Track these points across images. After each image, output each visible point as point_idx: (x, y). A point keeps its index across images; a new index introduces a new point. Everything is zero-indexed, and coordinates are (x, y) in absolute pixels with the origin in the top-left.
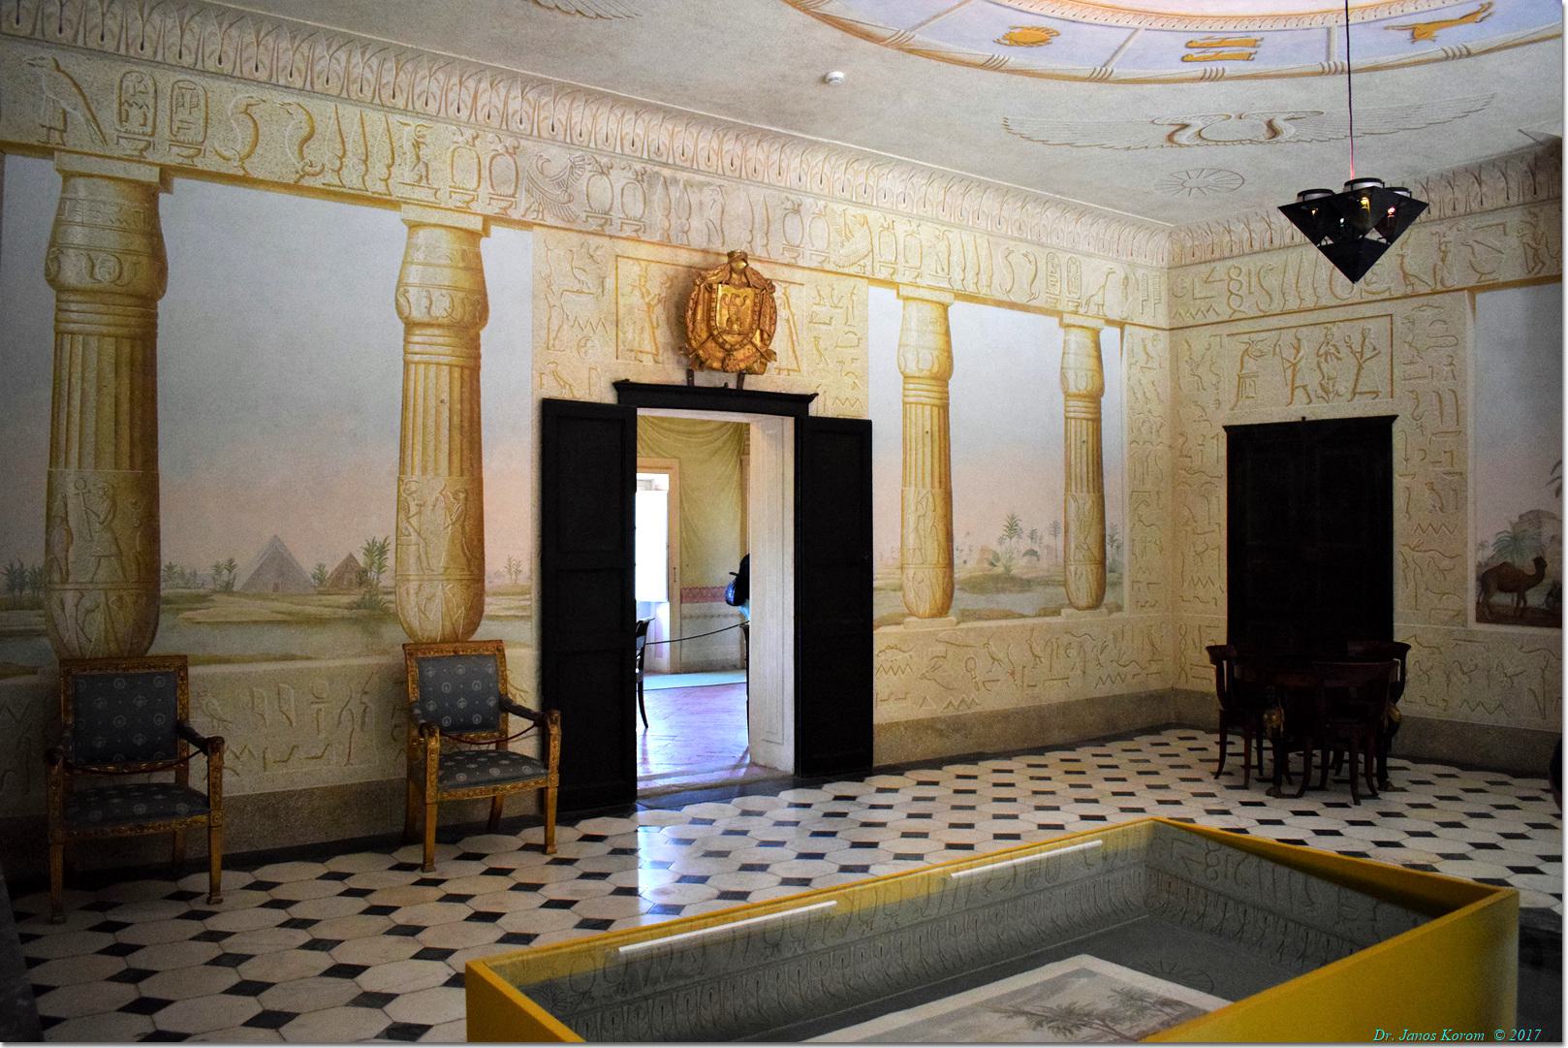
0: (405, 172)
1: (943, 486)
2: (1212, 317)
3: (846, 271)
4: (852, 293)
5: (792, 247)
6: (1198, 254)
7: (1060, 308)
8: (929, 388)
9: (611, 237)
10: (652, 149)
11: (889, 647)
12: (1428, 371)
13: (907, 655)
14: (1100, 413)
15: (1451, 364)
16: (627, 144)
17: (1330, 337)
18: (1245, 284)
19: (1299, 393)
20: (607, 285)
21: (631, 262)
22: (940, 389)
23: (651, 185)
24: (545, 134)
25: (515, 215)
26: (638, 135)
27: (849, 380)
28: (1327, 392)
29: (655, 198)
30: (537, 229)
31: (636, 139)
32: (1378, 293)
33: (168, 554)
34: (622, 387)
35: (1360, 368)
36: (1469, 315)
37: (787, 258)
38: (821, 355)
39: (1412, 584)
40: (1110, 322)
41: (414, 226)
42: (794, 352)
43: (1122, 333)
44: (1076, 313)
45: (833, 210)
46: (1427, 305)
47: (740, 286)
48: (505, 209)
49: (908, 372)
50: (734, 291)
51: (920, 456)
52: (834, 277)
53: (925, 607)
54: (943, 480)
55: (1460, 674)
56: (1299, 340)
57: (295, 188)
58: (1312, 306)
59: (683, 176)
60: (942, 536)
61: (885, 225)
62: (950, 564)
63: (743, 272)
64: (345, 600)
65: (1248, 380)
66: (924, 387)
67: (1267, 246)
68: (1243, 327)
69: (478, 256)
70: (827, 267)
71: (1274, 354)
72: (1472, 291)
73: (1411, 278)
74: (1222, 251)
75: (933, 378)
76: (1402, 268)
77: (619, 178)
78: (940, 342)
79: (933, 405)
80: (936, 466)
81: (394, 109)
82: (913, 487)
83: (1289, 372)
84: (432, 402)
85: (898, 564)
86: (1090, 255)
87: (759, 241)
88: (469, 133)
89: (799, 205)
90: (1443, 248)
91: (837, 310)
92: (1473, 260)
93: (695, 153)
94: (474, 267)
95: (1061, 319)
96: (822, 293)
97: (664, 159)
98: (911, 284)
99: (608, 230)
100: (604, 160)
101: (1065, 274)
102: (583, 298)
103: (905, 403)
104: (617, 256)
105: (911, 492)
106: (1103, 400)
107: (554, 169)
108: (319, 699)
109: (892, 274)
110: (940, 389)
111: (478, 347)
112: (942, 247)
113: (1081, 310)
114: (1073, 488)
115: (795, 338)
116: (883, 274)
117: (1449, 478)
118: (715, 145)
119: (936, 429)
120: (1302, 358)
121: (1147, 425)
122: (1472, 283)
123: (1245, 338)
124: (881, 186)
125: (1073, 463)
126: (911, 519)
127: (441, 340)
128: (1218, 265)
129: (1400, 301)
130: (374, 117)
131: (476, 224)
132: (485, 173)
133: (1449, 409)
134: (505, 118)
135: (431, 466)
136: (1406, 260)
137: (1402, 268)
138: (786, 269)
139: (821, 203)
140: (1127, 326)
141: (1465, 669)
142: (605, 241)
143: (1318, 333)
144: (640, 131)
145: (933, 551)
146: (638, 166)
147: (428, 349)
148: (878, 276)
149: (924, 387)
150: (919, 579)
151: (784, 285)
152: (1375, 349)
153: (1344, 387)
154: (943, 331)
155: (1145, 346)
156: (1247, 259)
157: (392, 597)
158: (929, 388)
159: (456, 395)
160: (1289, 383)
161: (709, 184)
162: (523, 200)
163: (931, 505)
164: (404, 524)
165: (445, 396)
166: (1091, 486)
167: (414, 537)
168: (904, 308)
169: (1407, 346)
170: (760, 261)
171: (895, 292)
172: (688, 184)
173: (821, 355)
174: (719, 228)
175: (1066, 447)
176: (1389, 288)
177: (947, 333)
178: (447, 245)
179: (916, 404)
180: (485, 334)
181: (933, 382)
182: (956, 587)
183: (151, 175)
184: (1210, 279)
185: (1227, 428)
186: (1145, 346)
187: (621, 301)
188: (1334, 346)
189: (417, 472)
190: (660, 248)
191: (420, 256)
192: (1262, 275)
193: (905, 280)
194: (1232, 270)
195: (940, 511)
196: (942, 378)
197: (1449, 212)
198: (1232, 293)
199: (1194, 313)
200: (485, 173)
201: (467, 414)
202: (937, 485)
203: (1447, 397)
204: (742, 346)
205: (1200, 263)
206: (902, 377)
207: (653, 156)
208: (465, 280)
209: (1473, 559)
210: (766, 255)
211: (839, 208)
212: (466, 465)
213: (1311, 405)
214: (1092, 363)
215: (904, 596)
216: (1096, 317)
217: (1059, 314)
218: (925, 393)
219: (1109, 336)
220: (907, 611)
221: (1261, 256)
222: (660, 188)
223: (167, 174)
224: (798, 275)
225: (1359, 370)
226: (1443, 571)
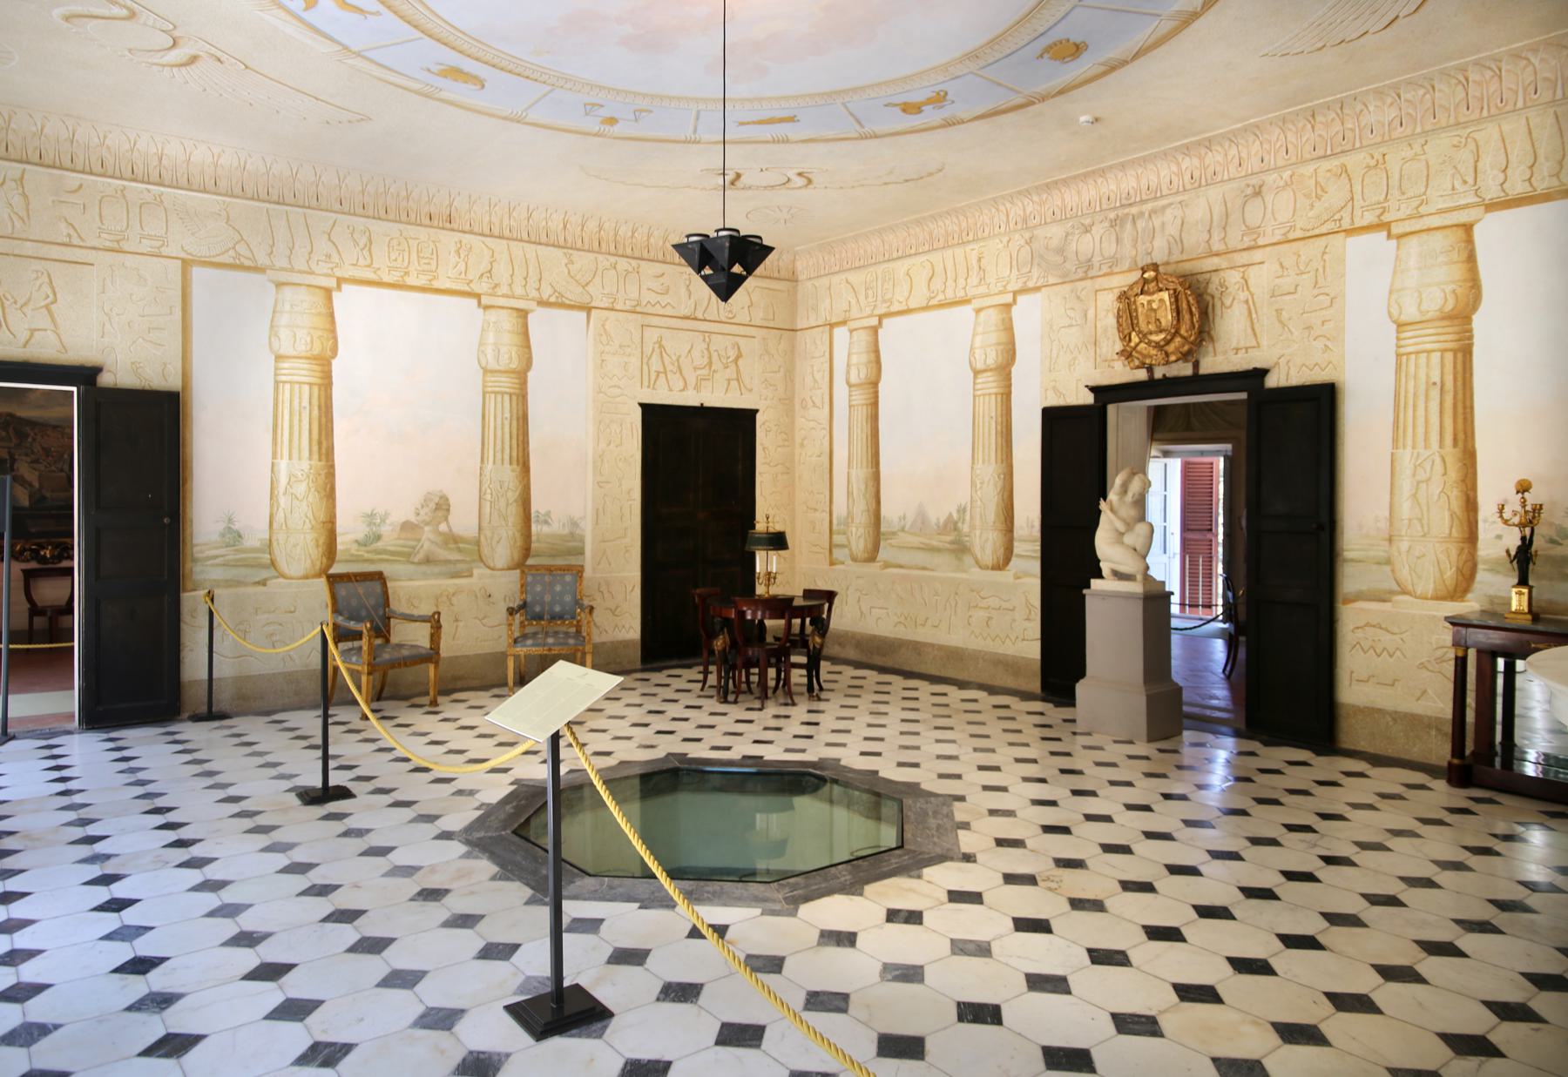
0: (974, 280)
1: (1461, 444)
3: (1317, 232)
4: (1324, 253)
5: (1251, 230)
8: (1440, 330)
9: (1092, 278)
10: (1123, 196)
11: (1368, 625)
13: (1397, 638)
16: (1104, 201)
20: (1089, 316)
21: (1106, 292)
22: (1456, 329)
23: (1122, 226)
24: (1048, 220)
25: (1031, 284)
26: (1112, 191)
27: (1319, 344)
29: (1125, 235)
30: (1043, 289)
31: (1111, 194)
33: (884, 511)
34: (1095, 390)
37: (1247, 242)
38: (1284, 325)
41: (978, 311)
42: (1253, 330)
45: (1302, 175)
47: (1153, 293)
48: (1025, 283)
49: (1404, 318)
50: (1148, 298)
51: (1421, 411)
52: (1302, 243)
53: (1427, 585)
54: (1461, 436)
57: (926, 308)
59: (1149, 206)
60: (1457, 505)
61: (1373, 163)
63: (1156, 279)
64: (948, 538)
66: (1432, 331)
69: (1011, 319)
70: (1291, 236)
75: (1443, 318)
77: (1098, 231)
78: (1458, 272)
79: (1444, 351)
81: (969, 242)
82: (1409, 449)
84: (987, 419)
85: (1387, 536)
87: (1216, 236)
88: (1005, 240)
89: (1260, 187)
91: (1305, 276)
93: (1159, 184)
94: (1009, 328)
96: (1284, 264)
97: (1132, 201)
98: (1410, 218)
99: (1091, 274)
100: (1087, 221)
102: (1074, 329)
104: (1097, 291)
107: (1054, 243)
108: (936, 594)
109: (1379, 216)
110: (1456, 329)
111: (1010, 379)
112: (1466, 156)
115: (1254, 316)
116: (1370, 218)
118: (1174, 168)
124: (1363, 124)
126: (1406, 486)
127: (991, 379)
130: (959, 251)
131: (1008, 298)
132: (1014, 263)
134: (1025, 220)
135: (986, 458)
138: (1245, 254)
139: (1286, 175)
142: (1088, 283)
144: (1113, 187)
145: (1442, 520)
146: (1112, 215)
147: (984, 385)
148: (1359, 223)
149: (1432, 331)
151: (1242, 269)
154: (1464, 255)
157: (967, 539)
158: (1440, 330)
159: (999, 413)
161: (1171, 204)
162: (1036, 273)
163: (1438, 467)
164: (974, 495)
165: (993, 414)
167: (979, 503)
168: (1398, 248)
170: (1217, 255)
171: (1385, 233)
172: (1153, 212)
173: (1284, 325)
174: (1178, 239)
177: (1471, 258)
178: (992, 317)
179: (1417, 353)
180: (1014, 370)
183: (874, 321)
187: (1098, 325)
189: (981, 461)
190: (1128, 274)
191: (980, 329)
193: (1401, 215)
195: (1454, 474)
200: (1014, 263)
201: (1004, 424)
204: (1168, 342)
206: (1395, 326)
207: (1124, 202)
208: (1003, 337)
210: (1224, 247)
211: (1308, 170)
212: (1004, 456)
215: (1393, 571)
218: (1433, 338)
220: (1396, 588)
222: (1129, 226)
223: (881, 318)
224: (1257, 255)
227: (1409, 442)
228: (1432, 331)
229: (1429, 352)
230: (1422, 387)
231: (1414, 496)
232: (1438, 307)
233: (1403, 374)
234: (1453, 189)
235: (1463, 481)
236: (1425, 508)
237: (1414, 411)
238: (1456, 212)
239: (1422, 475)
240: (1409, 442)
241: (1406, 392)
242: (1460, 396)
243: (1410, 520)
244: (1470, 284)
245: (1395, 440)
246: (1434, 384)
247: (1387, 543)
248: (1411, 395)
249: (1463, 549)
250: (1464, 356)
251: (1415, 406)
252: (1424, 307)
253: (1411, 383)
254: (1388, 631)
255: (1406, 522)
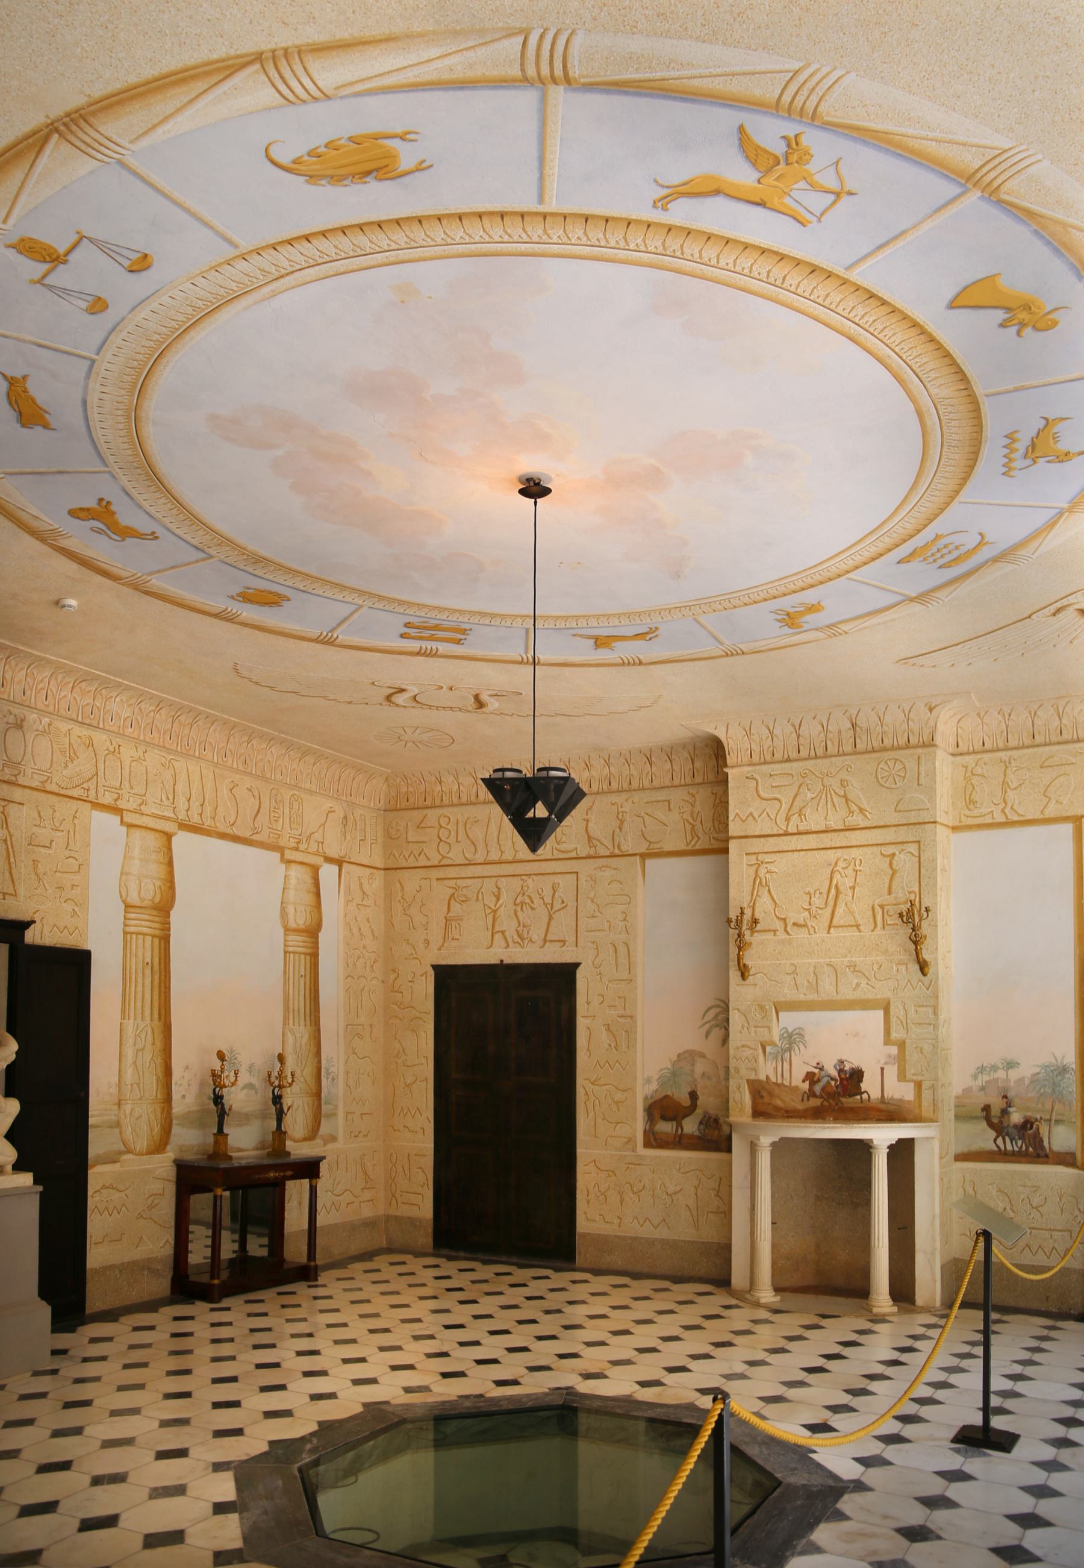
1: (163, 1019)
2: (422, 861)
6: (411, 800)
7: (281, 843)
11: (104, 1187)
12: (606, 926)
13: (122, 1194)
14: (317, 948)
15: (625, 920)
17: (525, 888)
18: (453, 834)
19: (498, 937)
28: (522, 939)
32: (567, 852)
35: (550, 918)
36: (640, 877)
39: (592, 1114)
40: (329, 860)
43: (340, 870)
44: (297, 849)
46: (607, 867)
51: (140, 988)
53: (142, 1144)
54: (163, 1012)
55: (631, 1195)
56: (499, 888)
58: (510, 858)
60: (160, 1071)
62: (168, 1099)
65: (454, 923)
66: (151, 918)
67: (473, 798)
68: (452, 872)
71: (477, 899)
72: (644, 856)
73: (594, 841)
74: (434, 799)
76: (587, 831)
79: (153, 936)
80: (156, 998)
83: (490, 917)
85: (117, 1101)
86: (311, 792)
90: (620, 816)
92: (644, 829)
95: (282, 855)
101: (287, 811)
103: (125, 933)
105: (130, 1025)
106: (320, 935)
113: (302, 847)
114: (291, 1022)
117: (621, 1020)
119: (156, 960)
120: (501, 906)
121: (361, 961)
122: (643, 850)
123: (452, 883)
125: (291, 996)
126: (130, 1053)
128: (429, 812)
129: (584, 861)
133: (623, 960)
136: (590, 825)
137: (587, 831)
140: (345, 865)
141: (635, 1190)
143: (516, 883)
149: (146, 917)
150: (136, 1115)
152: (563, 902)
153: (537, 934)
155: (361, 884)
156: (455, 809)
160: (490, 927)
166: (308, 1018)
169: (589, 901)
175: (285, 982)
176: (576, 849)
179: (138, 934)
181: (155, 913)
182: (174, 1122)
184: (423, 825)
185: (435, 967)
186: (361, 884)
188: (530, 897)
192: (468, 827)
194: (441, 819)
195: (159, 1044)
196: (164, 907)
197: (625, 786)
198: (441, 840)
199: (407, 856)
202: (156, 1016)
203: (622, 949)
205: (414, 809)
209: (644, 1090)
213: (509, 950)
214: (309, 899)
215: (121, 1133)
216: (317, 854)
217: (281, 850)
218: (147, 923)
219: (328, 873)
220: (123, 1148)
221: (467, 807)
225: (550, 920)
226: (617, 1103)
227: (132, 1015)
228: (146, 917)
229: (144, 935)
230: (141, 966)
231: (135, 1062)
232: (151, 898)
233: (128, 951)
234: (161, 800)
235: (164, 1050)
236: (141, 1074)
237: (136, 986)
238: (162, 821)
239: (140, 1046)
240: (132, 1015)
241: (130, 968)
242: (163, 977)
243: (132, 1085)
244: (169, 885)
245: (123, 1011)
246: (147, 964)
247: (117, 1107)
248: (133, 971)
249: (164, 1108)
250: (165, 944)
251: (136, 981)
252: (142, 895)
253: (134, 959)
254: (117, 1190)
255: (129, 1086)
